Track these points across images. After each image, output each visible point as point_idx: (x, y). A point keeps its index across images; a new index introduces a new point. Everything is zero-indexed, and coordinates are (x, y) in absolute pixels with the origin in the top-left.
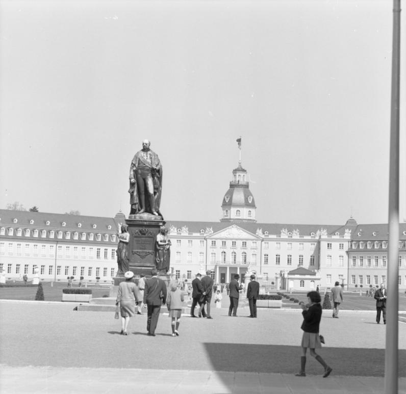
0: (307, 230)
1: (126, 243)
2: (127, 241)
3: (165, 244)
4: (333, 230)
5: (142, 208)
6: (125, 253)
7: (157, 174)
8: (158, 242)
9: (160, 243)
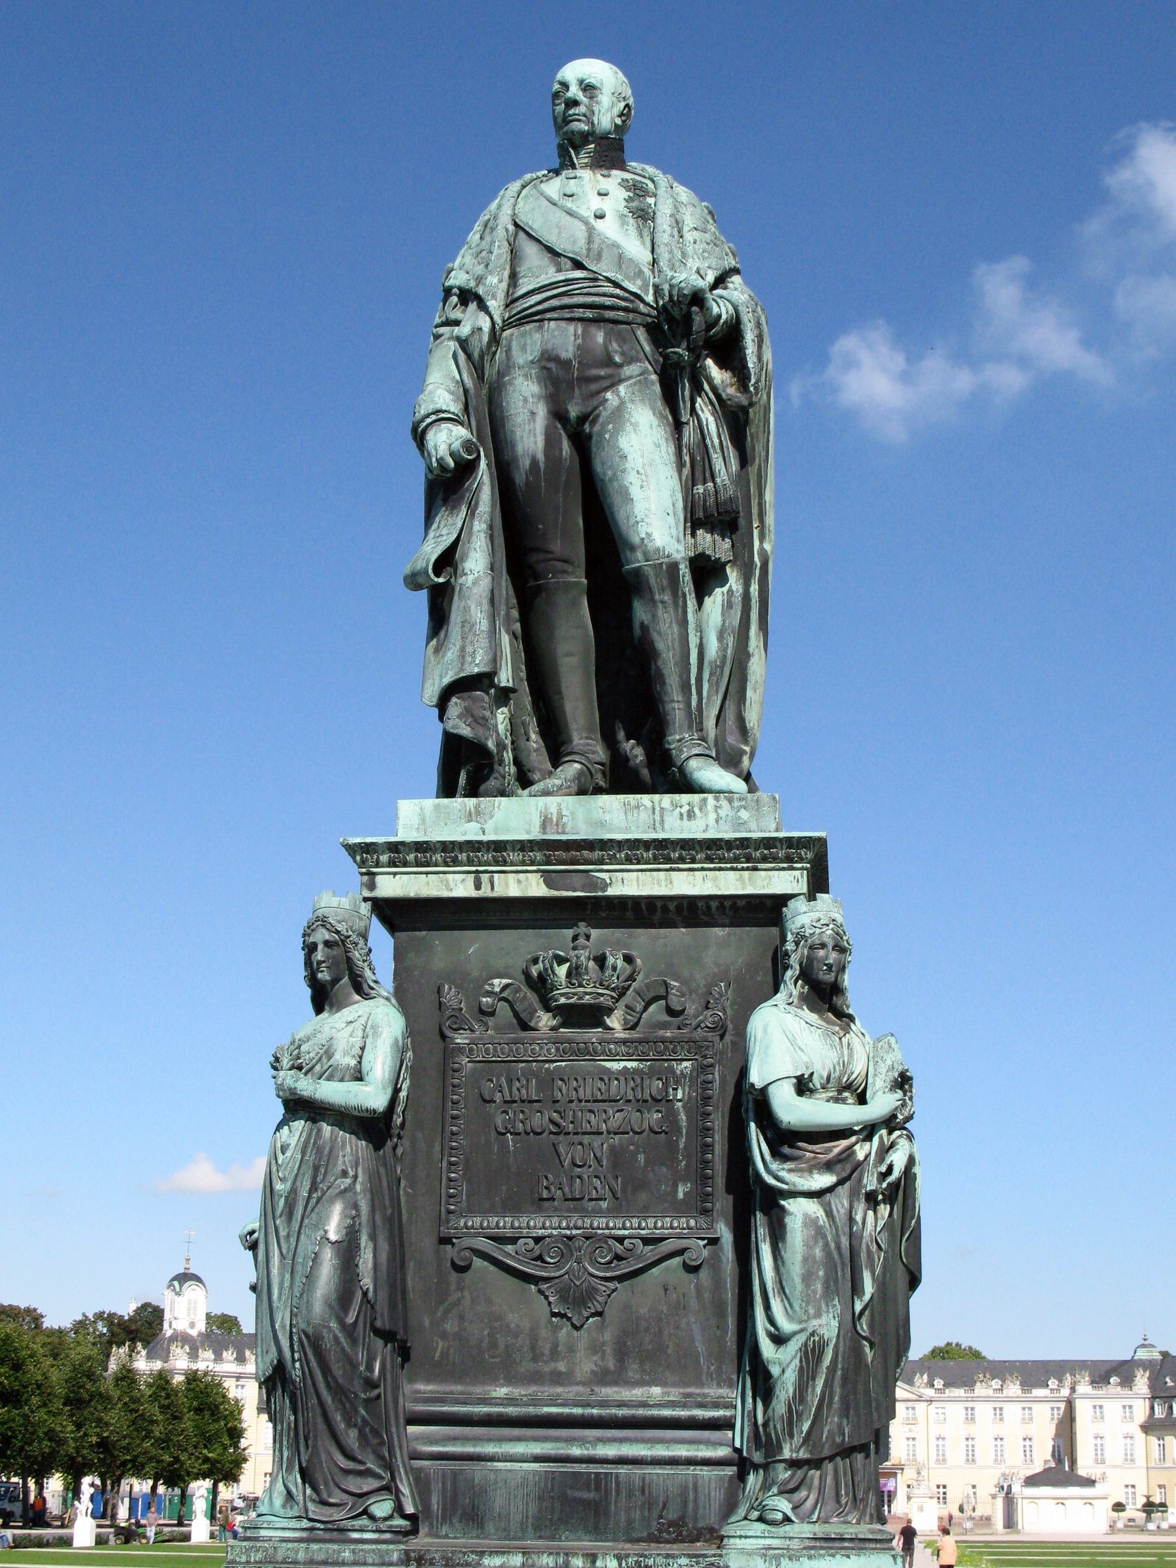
0: (1034, 1374)
1: (373, 1127)
2: (372, 1096)
3: (846, 1114)
4: (1105, 1373)
5: (557, 752)
6: (348, 1250)
7: (716, 373)
8: (761, 1106)
9: (791, 1109)
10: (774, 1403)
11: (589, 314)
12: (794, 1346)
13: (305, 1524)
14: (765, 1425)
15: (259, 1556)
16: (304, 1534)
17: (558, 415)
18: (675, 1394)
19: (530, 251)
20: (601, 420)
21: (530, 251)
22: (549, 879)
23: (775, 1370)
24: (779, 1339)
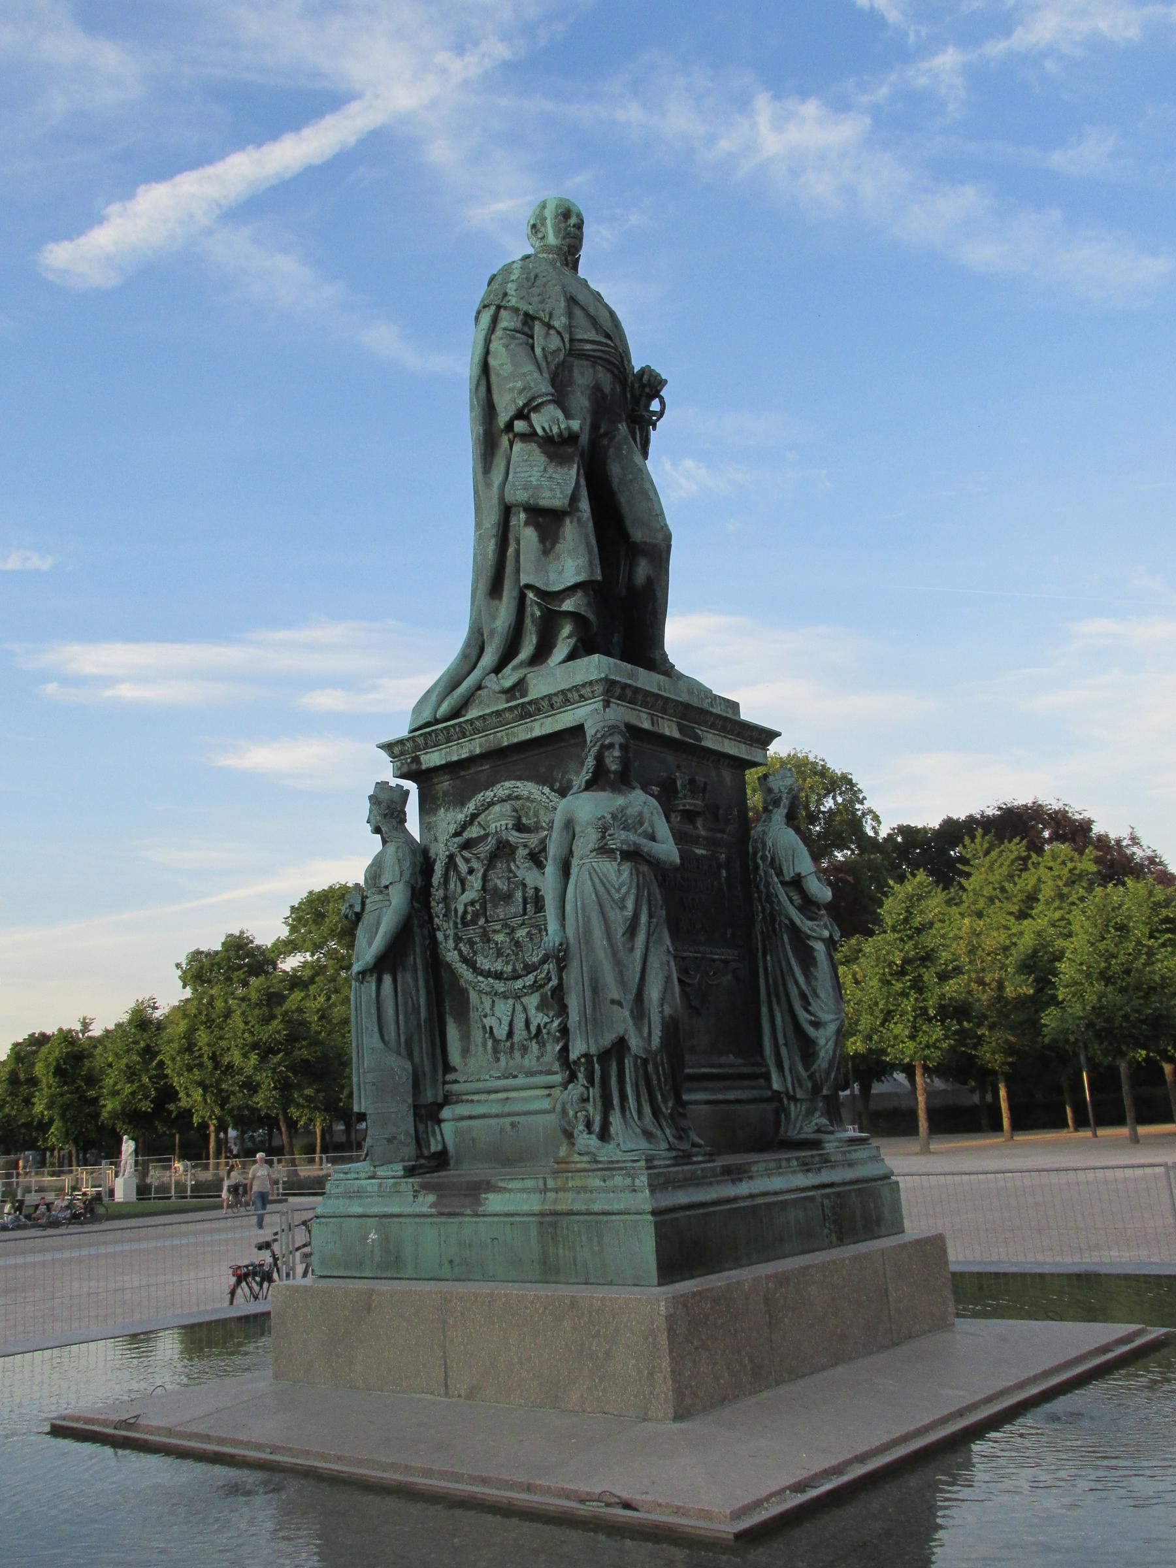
10: (818, 1062)
11: (616, 372)
12: (832, 1028)
13: (674, 1154)
14: (811, 1077)
15: (662, 1180)
16: (707, 1158)
17: (595, 427)
18: (740, 1061)
19: (578, 313)
20: (617, 439)
21: (578, 313)
22: (681, 729)
23: (822, 1042)
24: (816, 1025)
